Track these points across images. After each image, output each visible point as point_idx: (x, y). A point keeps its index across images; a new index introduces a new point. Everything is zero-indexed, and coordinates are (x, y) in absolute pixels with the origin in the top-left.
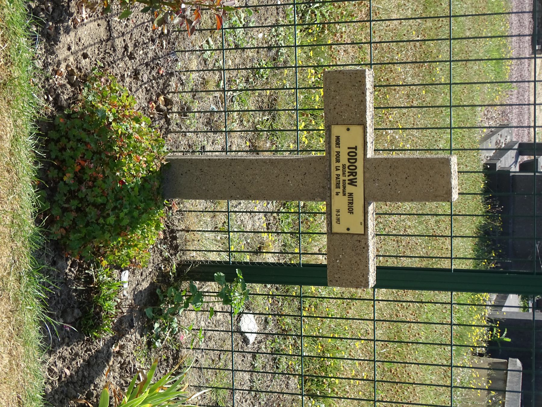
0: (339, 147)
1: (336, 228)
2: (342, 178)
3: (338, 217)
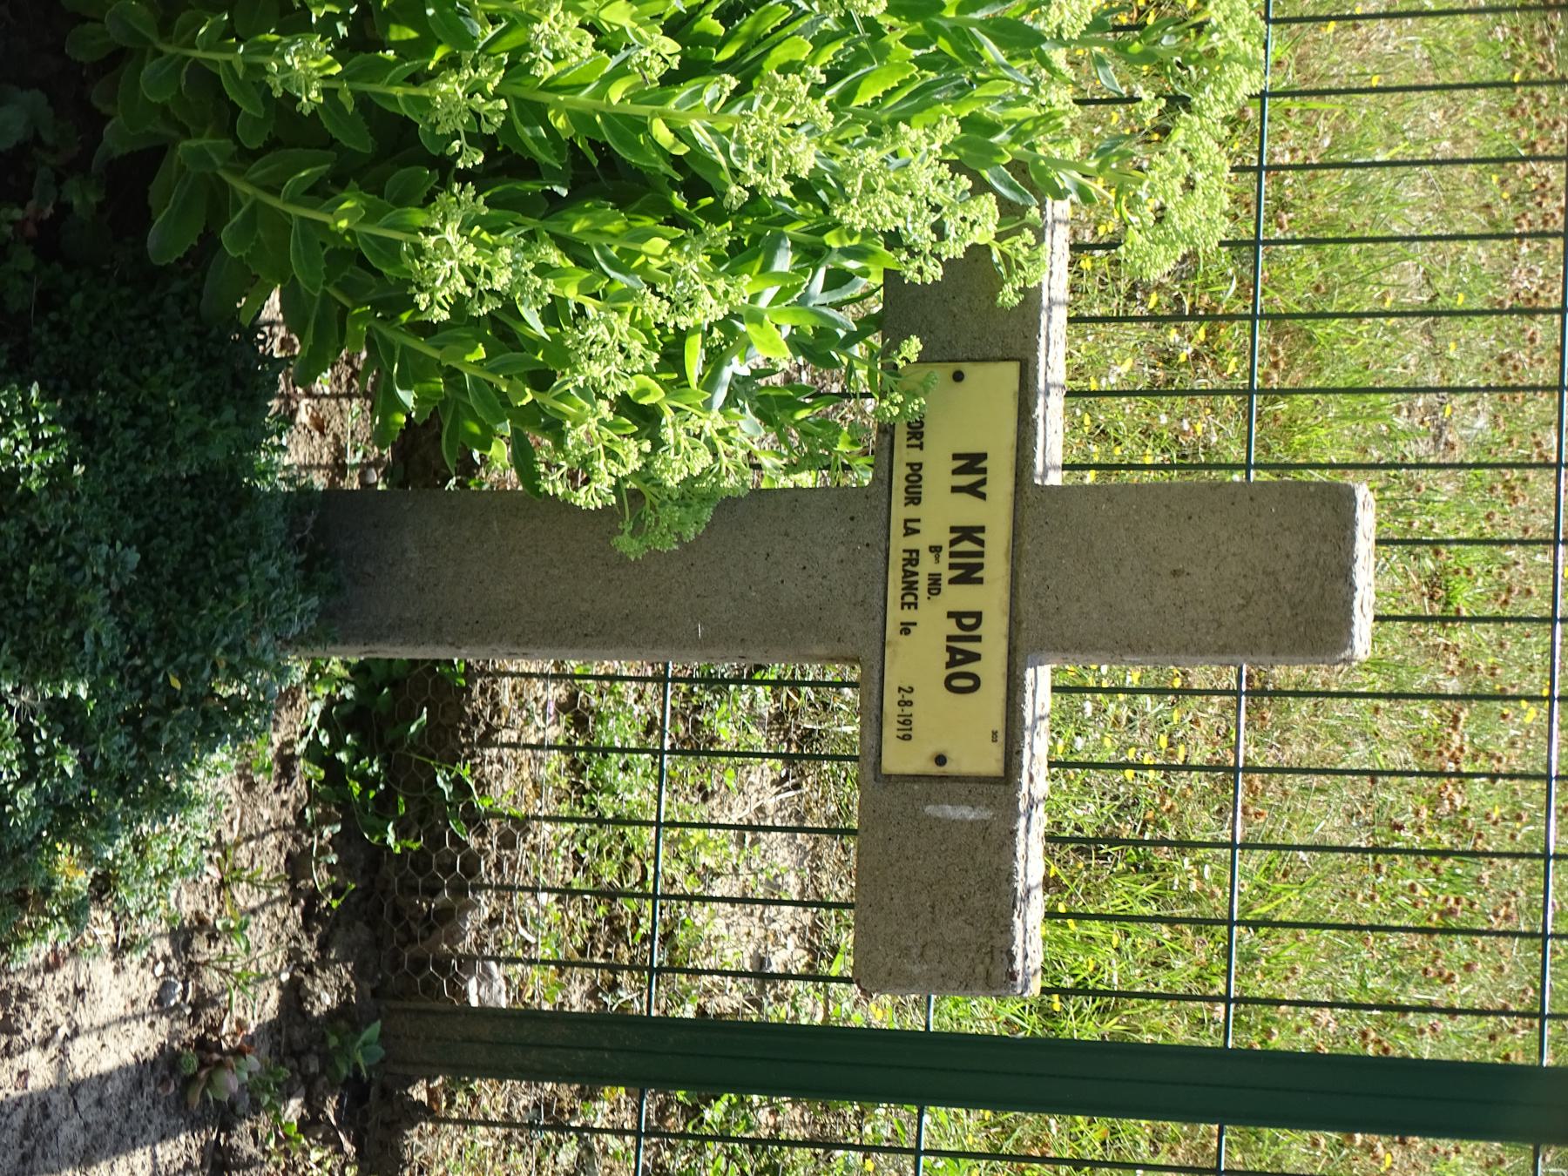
0: (921, 447)
1: (900, 758)
2: (927, 565)
3: (908, 710)
